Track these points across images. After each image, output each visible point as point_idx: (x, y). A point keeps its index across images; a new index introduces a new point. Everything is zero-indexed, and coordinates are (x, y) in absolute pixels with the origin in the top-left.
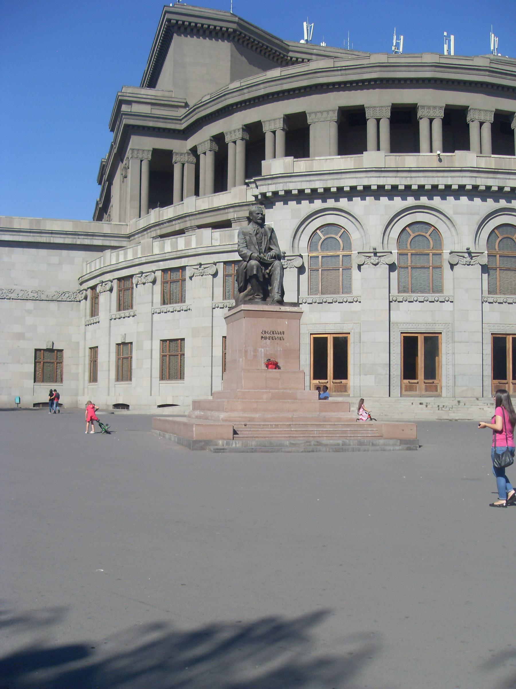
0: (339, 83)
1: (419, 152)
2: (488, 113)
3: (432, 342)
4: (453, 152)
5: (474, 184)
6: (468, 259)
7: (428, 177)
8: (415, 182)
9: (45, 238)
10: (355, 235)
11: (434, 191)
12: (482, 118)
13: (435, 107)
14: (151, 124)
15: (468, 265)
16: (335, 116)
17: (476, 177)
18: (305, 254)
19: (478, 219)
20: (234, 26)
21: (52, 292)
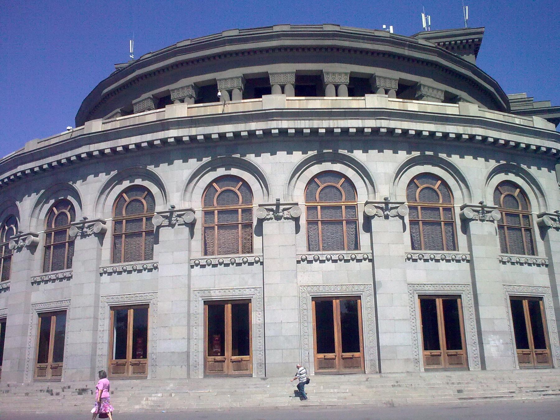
2: (235, 80)
5: (88, 151)
12: (229, 85)
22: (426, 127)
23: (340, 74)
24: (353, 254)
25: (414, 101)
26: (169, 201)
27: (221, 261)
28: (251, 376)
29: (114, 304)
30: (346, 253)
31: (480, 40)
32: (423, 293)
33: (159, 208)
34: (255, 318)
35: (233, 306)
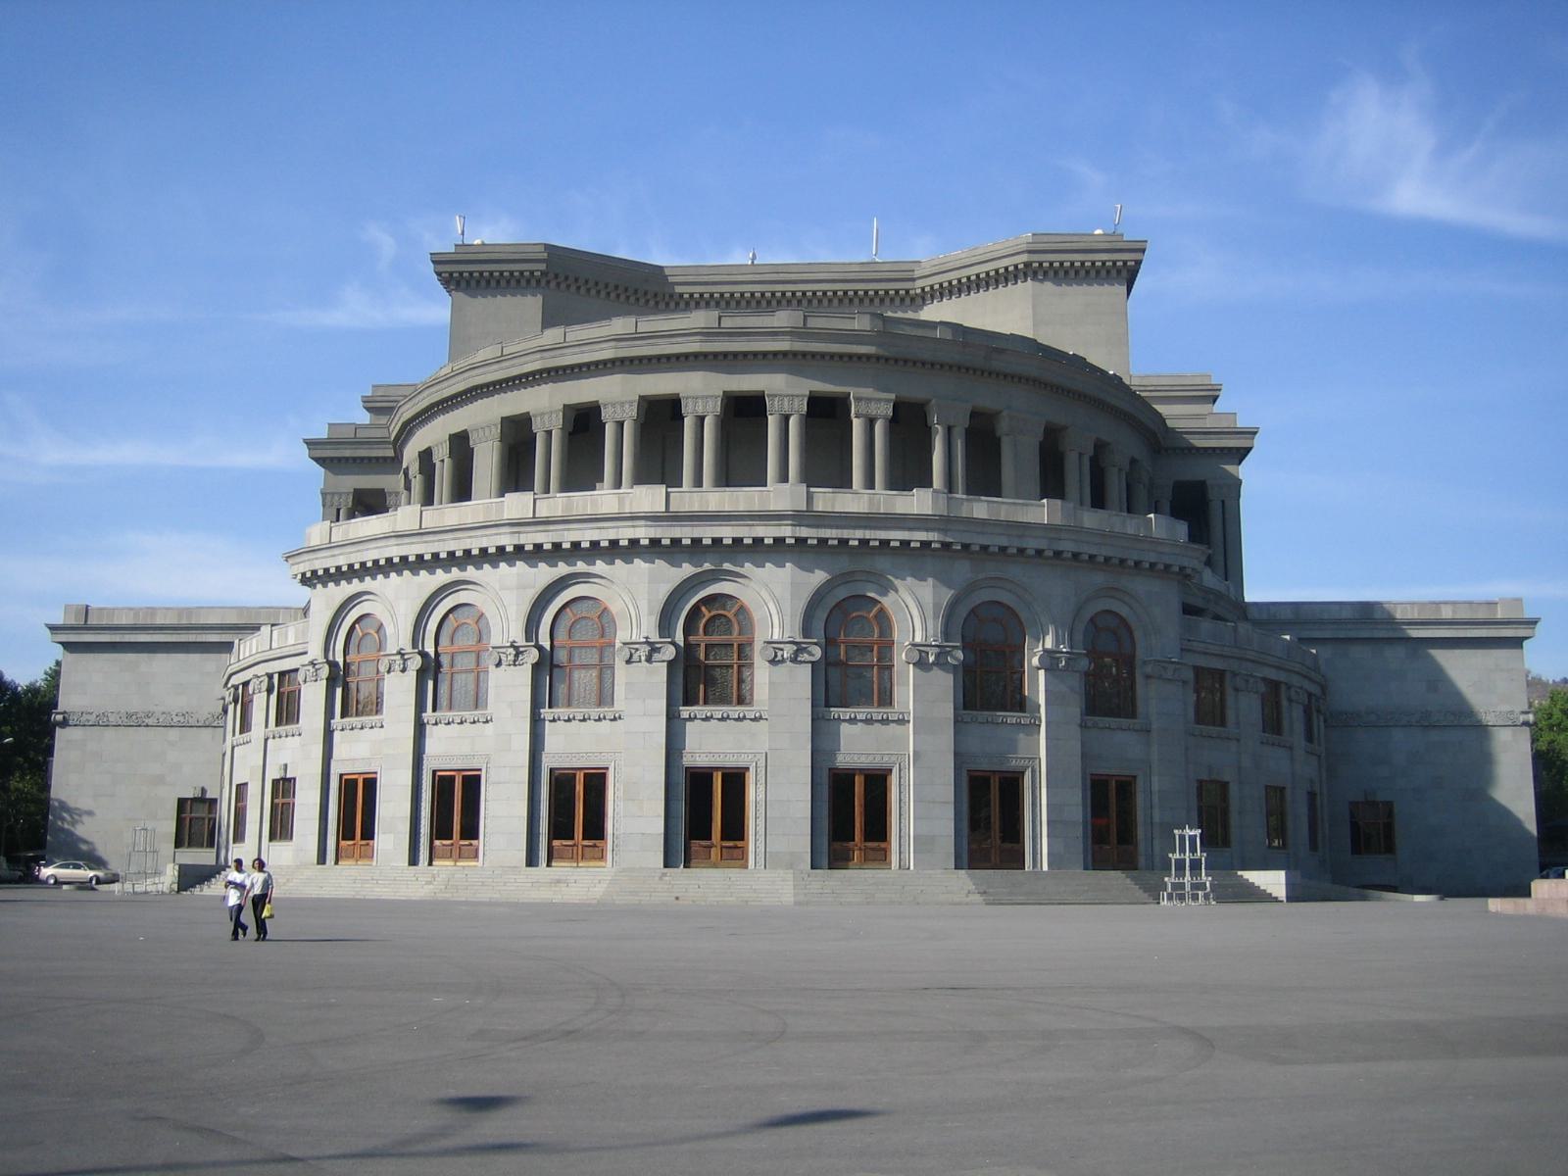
0: (500, 382)
1: (469, 499)
3: (472, 784)
4: (503, 496)
5: (516, 543)
6: (511, 658)
7: (459, 539)
8: (443, 547)
9: (194, 636)
10: (389, 630)
11: (468, 558)
12: (700, 411)
13: (622, 404)
14: (347, 453)
15: (515, 665)
16: (497, 431)
17: (519, 533)
18: (340, 659)
19: (531, 594)
20: (543, 266)
21: (203, 715)
22: (996, 541)
23: (879, 400)
24: (885, 713)
25: (983, 498)
26: (639, 626)
27: (709, 714)
28: (747, 867)
29: (555, 765)
30: (877, 712)
31: (1138, 263)
32: (973, 767)
33: (622, 636)
34: (753, 793)
35: (724, 776)
